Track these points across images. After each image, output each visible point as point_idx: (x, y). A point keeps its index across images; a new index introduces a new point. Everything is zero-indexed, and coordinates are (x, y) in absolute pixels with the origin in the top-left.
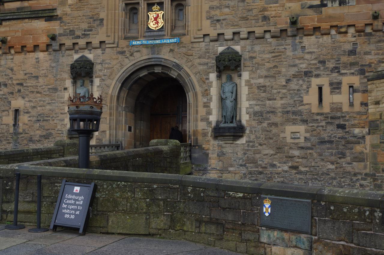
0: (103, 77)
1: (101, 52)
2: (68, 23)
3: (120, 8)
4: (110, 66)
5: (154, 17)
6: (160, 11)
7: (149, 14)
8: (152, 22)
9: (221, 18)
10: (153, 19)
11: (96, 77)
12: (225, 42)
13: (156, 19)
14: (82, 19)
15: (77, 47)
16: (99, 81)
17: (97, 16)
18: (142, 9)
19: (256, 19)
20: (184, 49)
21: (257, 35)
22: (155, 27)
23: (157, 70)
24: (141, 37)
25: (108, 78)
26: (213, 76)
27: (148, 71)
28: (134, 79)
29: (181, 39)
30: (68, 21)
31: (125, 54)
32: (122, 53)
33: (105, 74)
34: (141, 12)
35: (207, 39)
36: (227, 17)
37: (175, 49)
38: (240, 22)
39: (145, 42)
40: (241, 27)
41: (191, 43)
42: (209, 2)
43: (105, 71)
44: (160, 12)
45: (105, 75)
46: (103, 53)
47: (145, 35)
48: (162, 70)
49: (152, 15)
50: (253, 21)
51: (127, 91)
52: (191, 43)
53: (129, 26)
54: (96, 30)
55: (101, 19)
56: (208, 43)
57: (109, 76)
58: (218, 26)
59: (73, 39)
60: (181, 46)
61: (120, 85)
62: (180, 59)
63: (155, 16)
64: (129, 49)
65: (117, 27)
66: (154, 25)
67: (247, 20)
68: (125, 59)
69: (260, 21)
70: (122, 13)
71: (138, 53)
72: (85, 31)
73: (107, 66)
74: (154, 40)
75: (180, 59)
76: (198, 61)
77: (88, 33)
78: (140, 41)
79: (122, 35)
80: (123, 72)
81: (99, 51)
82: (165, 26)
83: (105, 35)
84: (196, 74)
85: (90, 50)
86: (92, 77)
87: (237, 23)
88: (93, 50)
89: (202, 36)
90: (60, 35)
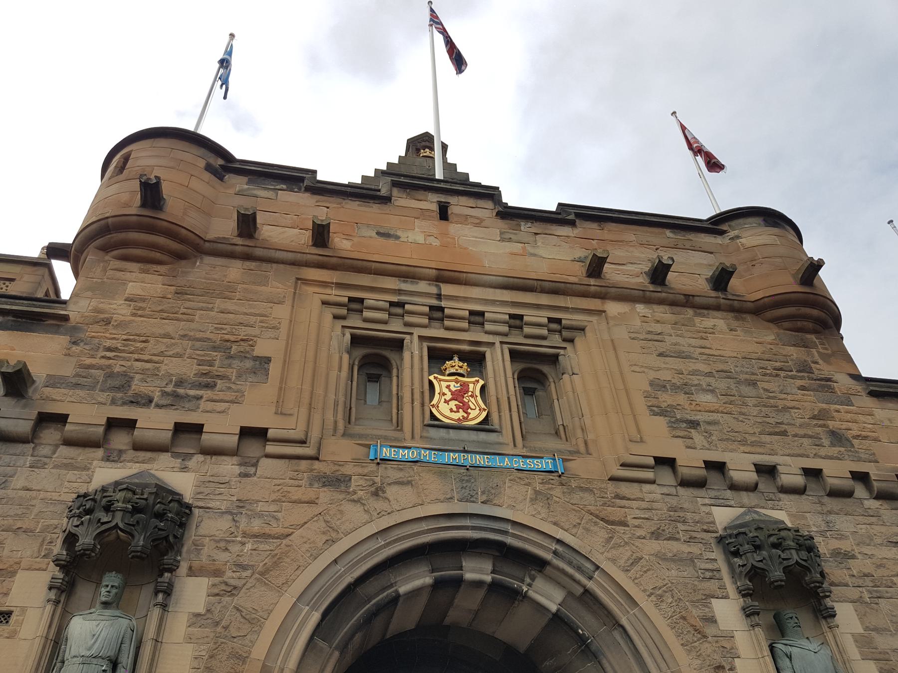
0: (229, 575)
1: (237, 470)
2: (109, 349)
3: (335, 343)
4: (276, 529)
5: (453, 389)
7: (432, 378)
8: (446, 402)
9: (699, 417)
10: (449, 396)
11: (191, 572)
12: (729, 494)
14: (174, 344)
15: (120, 440)
16: (204, 593)
17: (244, 346)
19: (810, 437)
20: (588, 498)
21: (832, 482)
23: (473, 571)
25: (258, 580)
26: (728, 611)
27: (433, 571)
28: (369, 601)
29: (568, 464)
30: (108, 343)
31: (348, 487)
32: (337, 482)
33: (245, 561)
35: (666, 476)
36: (716, 417)
38: (767, 439)
40: (773, 453)
41: (612, 479)
42: (646, 370)
43: (249, 546)
44: (473, 379)
45: (244, 568)
46: (246, 475)
47: (425, 434)
48: (493, 572)
49: (445, 385)
50: (806, 441)
51: (337, 654)
52: (612, 479)
54: (233, 386)
55: (256, 358)
56: (673, 491)
57: (262, 574)
58: (698, 438)
59: (113, 402)
61: (316, 617)
62: (581, 531)
63: (454, 387)
64: (366, 471)
65: (320, 391)
67: (784, 433)
68: (348, 507)
69: (826, 442)
70: (341, 358)
71: (408, 489)
72: (180, 383)
73: (256, 526)
75: (581, 531)
76: (654, 546)
77: (192, 392)
78: (410, 448)
79: (336, 422)
80: (335, 561)
81: (228, 467)
83: (274, 409)
84: (661, 596)
85: (186, 457)
86: (172, 569)
87: (754, 439)
88: (200, 458)
89: (651, 461)
90: (53, 381)
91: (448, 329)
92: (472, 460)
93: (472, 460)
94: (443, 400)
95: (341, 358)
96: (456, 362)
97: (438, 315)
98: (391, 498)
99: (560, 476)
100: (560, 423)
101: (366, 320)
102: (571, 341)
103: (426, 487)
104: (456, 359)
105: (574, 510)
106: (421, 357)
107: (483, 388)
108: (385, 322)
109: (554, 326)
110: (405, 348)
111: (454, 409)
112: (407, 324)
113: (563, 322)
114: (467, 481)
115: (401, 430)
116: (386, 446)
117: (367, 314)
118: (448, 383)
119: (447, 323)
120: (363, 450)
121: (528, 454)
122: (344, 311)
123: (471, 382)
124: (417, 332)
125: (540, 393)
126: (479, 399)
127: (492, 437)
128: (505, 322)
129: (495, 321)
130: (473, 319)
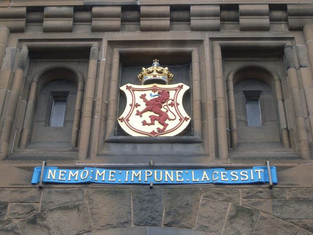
5: (149, 98)
6: (169, 84)
7: (123, 88)
8: (139, 114)
10: (143, 106)
13: (154, 106)
18: (98, 66)
22: (153, 133)
24: (88, 156)
29: (285, 173)
34: (97, 76)
37: (258, 208)
39: (102, 175)
47: (105, 152)
53: (32, 128)
60: (288, 195)
63: (150, 96)
64: (25, 196)
66: (144, 123)
70: (13, 75)
71: (75, 213)
74: (153, 167)
82: (203, 125)
91: (144, 30)
92: (158, 177)
93: (158, 177)
94: (135, 112)
95: (13, 75)
96: (155, 67)
97: (133, 15)
98: (51, 226)
99: (271, 187)
100: (284, 126)
101: (46, 30)
102: (300, 29)
103: (95, 211)
104: (156, 63)
105: (285, 226)
106: (110, 66)
107: (187, 96)
108: (70, 30)
109: (278, 14)
110: (91, 56)
111: (149, 121)
112: (95, 30)
113: (289, 7)
114: (149, 201)
115: (77, 151)
116: (51, 167)
117: (49, 23)
118: (143, 93)
119: (144, 23)
120: (26, 173)
121: (234, 165)
122: (21, 23)
123: (172, 89)
124: (107, 37)
125: (265, 96)
126: (181, 108)
127: (191, 149)
128: (215, 15)
129: (202, 15)
130: (176, 15)
